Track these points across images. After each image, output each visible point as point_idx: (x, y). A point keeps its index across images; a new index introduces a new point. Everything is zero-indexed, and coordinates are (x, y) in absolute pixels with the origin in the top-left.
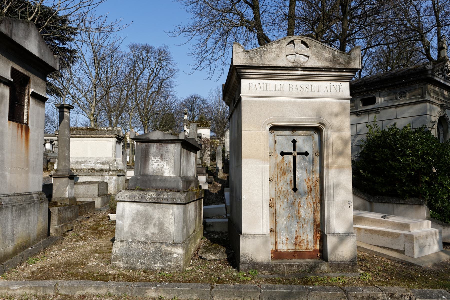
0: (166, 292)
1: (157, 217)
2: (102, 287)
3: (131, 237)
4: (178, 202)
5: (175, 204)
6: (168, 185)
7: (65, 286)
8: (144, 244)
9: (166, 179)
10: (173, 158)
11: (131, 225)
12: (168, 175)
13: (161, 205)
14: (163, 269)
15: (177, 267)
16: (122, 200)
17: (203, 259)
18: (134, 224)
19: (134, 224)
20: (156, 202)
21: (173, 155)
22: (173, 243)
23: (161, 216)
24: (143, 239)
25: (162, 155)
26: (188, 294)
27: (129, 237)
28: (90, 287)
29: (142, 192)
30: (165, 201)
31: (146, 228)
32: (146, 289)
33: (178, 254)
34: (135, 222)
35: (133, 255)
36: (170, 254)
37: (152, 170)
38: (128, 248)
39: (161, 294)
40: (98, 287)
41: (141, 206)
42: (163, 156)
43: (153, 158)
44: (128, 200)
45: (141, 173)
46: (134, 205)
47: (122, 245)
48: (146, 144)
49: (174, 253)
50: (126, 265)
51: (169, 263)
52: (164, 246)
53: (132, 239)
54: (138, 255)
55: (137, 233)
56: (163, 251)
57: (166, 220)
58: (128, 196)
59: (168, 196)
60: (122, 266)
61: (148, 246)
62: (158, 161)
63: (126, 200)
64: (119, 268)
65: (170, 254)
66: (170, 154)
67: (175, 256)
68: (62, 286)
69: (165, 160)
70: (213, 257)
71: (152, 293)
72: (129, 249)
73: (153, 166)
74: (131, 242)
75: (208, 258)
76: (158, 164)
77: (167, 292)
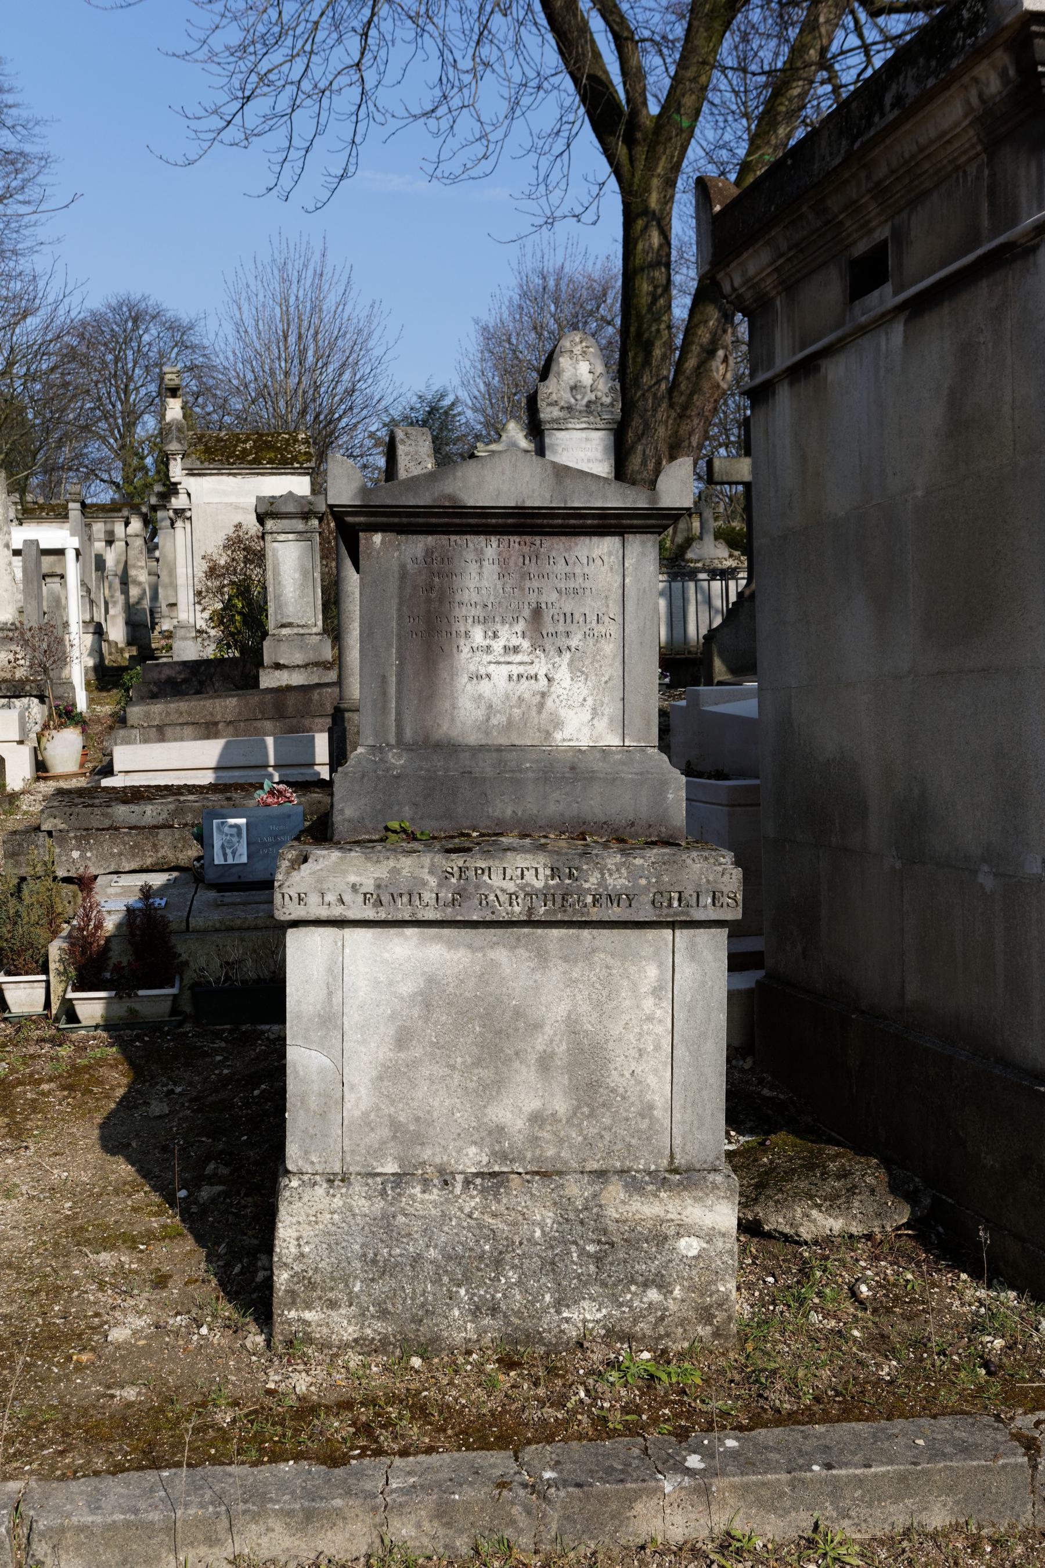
0: (760, 1503)
1: (561, 1010)
2: (338, 1512)
3: (393, 1148)
4: (699, 915)
5: (673, 925)
6: (595, 804)
7: (81, 1529)
8: (483, 1191)
9: (575, 770)
10: (614, 629)
11: (390, 1074)
12: (584, 741)
13: (586, 933)
14: (613, 1334)
15: (706, 1315)
16: (324, 913)
17: (768, 1236)
18: (413, 1064)
19: (413, 1064)
20: (560, 914)
21: (614, 610)
22: (675, 1171)
23: (585, 1008)
24: (473, 1158)
25: (537, 613)
26: (897, 1499)
27: (378, 1153)
28: (256, 1517)
29: (458, 861)
30: (615, 913)
31: (492, 1089)
32: (631, 1499)
33: (710, 1236)
34: (418, 1052)
35: (417, 1260)
36: (660, 1238)
37: (480, 714)
38: (386, 1221)
39: (730, 1516)
40: (309, 1516)
41: (451, 945)
42: (547, 619)
43: (478, 635)
44: (370, 914)
45: (408, 734)
46: (405, 948)
47: (338, 1202)
48: (430, 539)
49: (684, 1230)
50: (378, 1325)
51: (653, 1295)
52: (615, 1192)
53: (400, 1160)
54: (449, 1258)
55: (430, 1123)
56: (612, 1227)
57: (616, 1029)
58: (369, 885)
59: (634, 874)
60: (349, 1332)
61: (516, 1196)
62: (516, 650)
63: (352, 914)
64: (333, 1351)
65: (660, 1238)
66: (591, 606)
67: (689, 1246)
68: (62, 1530)
69: (562, 642)
70: (835, 1224)
71: (668, 1514)
72: (389, 1228)
73: (485, 688)
74: (399, 1179)
75: (806, 1233)
76: (516, 670)
77: (770, 1502)
